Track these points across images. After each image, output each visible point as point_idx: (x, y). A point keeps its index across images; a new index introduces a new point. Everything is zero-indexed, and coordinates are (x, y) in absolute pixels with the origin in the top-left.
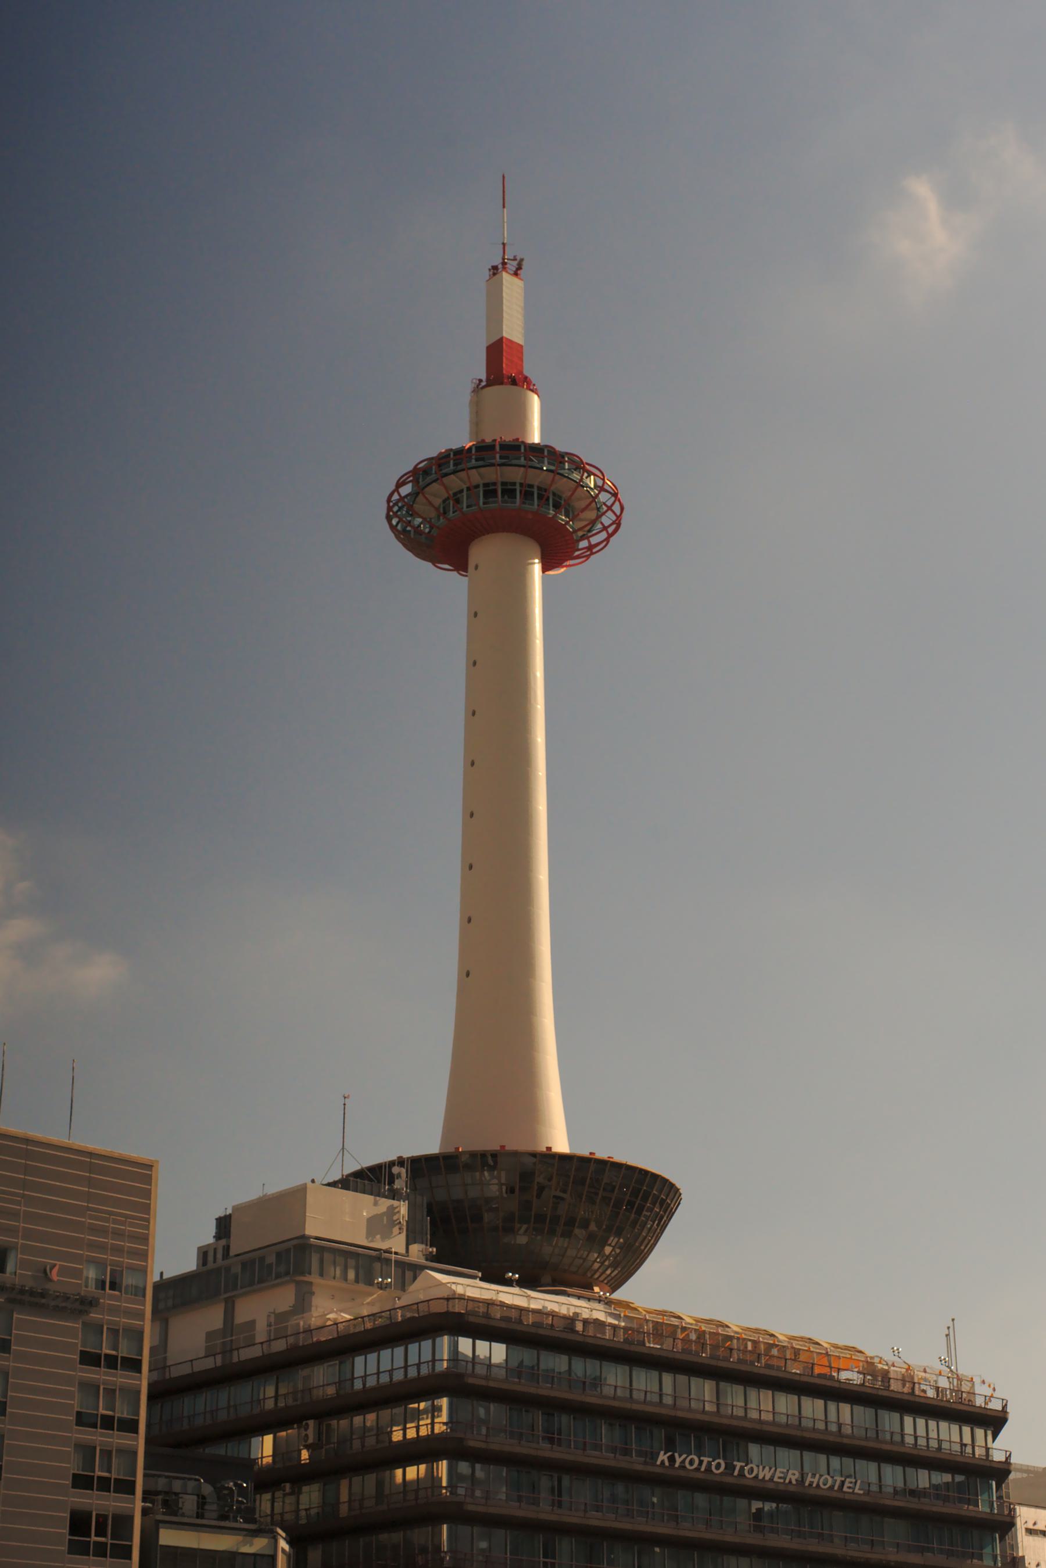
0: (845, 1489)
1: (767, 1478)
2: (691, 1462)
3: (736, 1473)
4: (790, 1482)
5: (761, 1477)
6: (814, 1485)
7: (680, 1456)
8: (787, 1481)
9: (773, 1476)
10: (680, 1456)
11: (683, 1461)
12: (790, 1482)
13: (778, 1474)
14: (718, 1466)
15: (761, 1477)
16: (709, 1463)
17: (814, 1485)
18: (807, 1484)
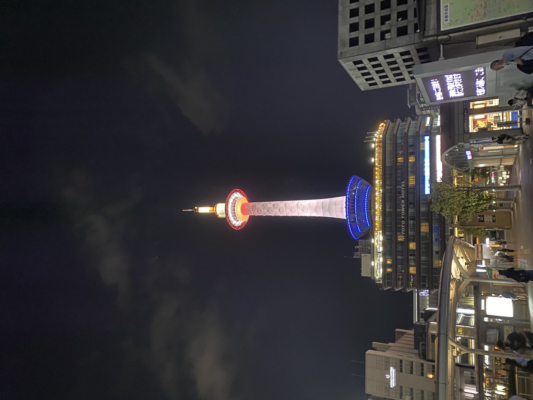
0: (404, 186)
1: (404, 209)
2: (403, 230)
3: (404, 217)
4: (404, 202)
5: (404, 211)
6: (404, 195)
7: (402, 233)
8: (404, 203)
9: (404, 207)
10: (402, 233)
11: (403, 232)
12: (404, 202)
13: (403, 206)
14: (403, 223)
15: (404, 211)
16: (403, 225)
17: (404, 195)
18: (404, 197)
